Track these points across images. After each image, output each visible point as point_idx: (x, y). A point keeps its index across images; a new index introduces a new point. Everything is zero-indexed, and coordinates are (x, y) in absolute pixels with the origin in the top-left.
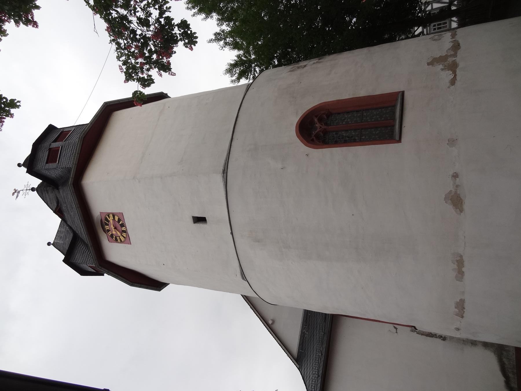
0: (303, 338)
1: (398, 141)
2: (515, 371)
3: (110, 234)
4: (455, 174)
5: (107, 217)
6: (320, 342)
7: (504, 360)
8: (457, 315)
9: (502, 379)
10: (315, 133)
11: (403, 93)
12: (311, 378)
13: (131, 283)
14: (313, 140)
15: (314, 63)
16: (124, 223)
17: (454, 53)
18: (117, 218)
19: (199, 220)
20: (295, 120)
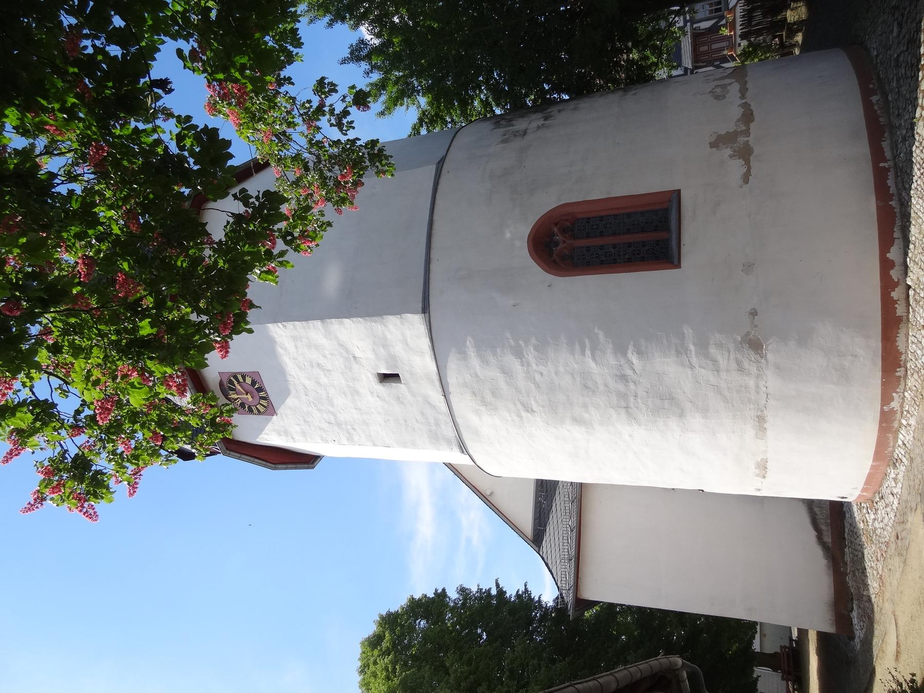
0: (539, 509)
1: (676, 266)
2: (829, 521)
3: (239, 403)
4: (753, 311)
5: (232, 378)
6: (568, 514)
7: (816, 509)
8: (758, 475)
9: (813, 533)
10: (556, 250)
11: (679, 191)
12: (558, 563)
13: (274, 466)
14: (554, 261)
15: (539, 127)
16: (262, 387)
17: (745, 128)
18: (249, 380)
19: (387, 378)
20: (526, 230)
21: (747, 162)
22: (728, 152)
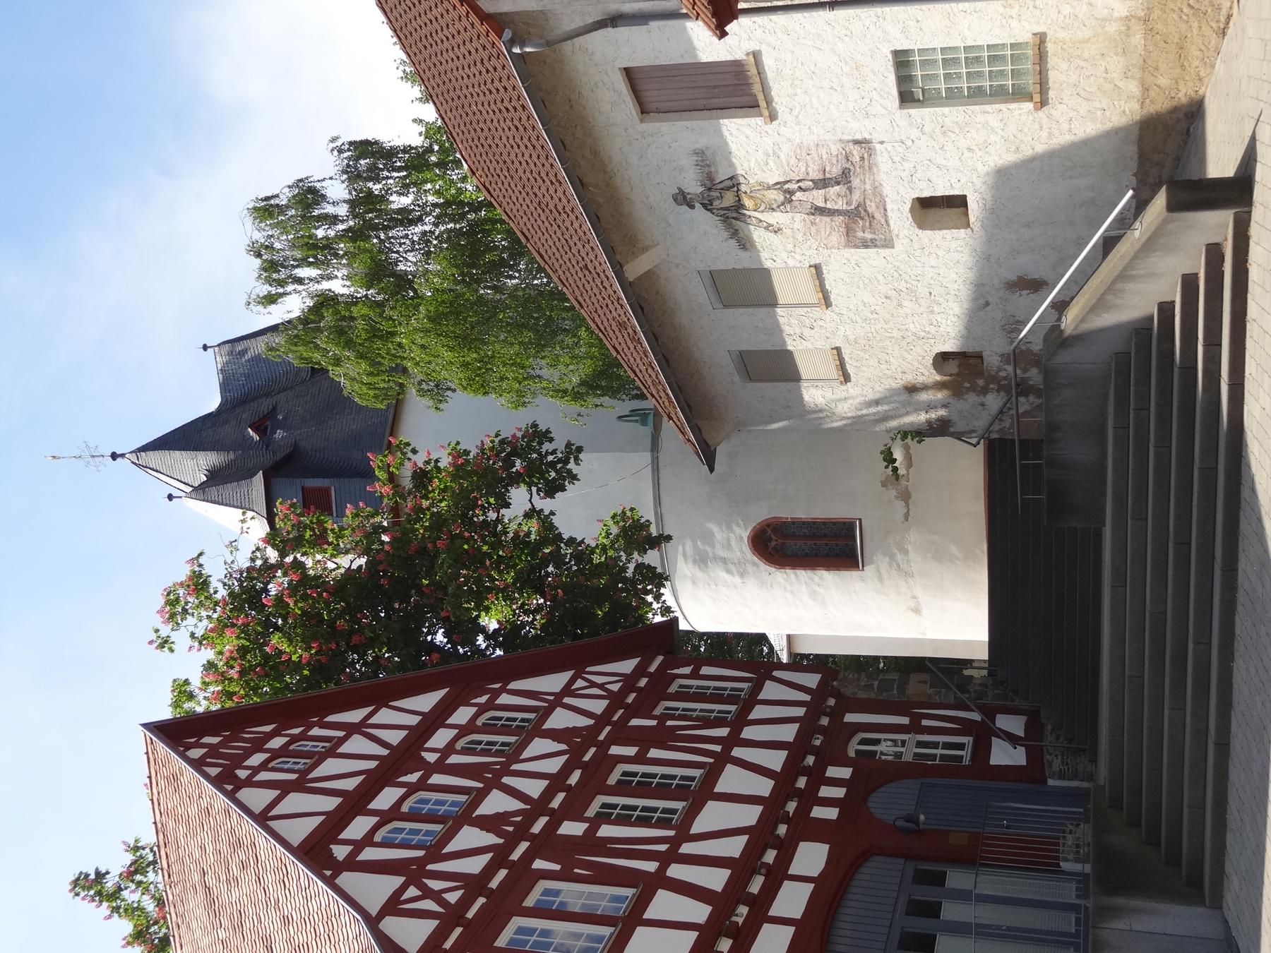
11: (860, 520)
20: (746, 534)
21: (907, 505)
22: (894, 493)
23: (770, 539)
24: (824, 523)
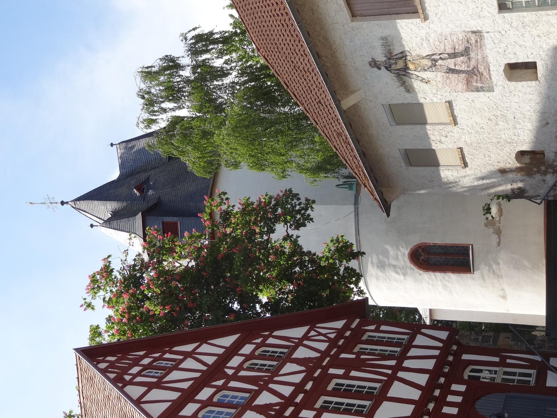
11: (472, 245)
14: (420, 263)
20: (407, 252)
21: (499, 237)
22: (491, 230)
23: (421, 255)
24: (452, 247)
